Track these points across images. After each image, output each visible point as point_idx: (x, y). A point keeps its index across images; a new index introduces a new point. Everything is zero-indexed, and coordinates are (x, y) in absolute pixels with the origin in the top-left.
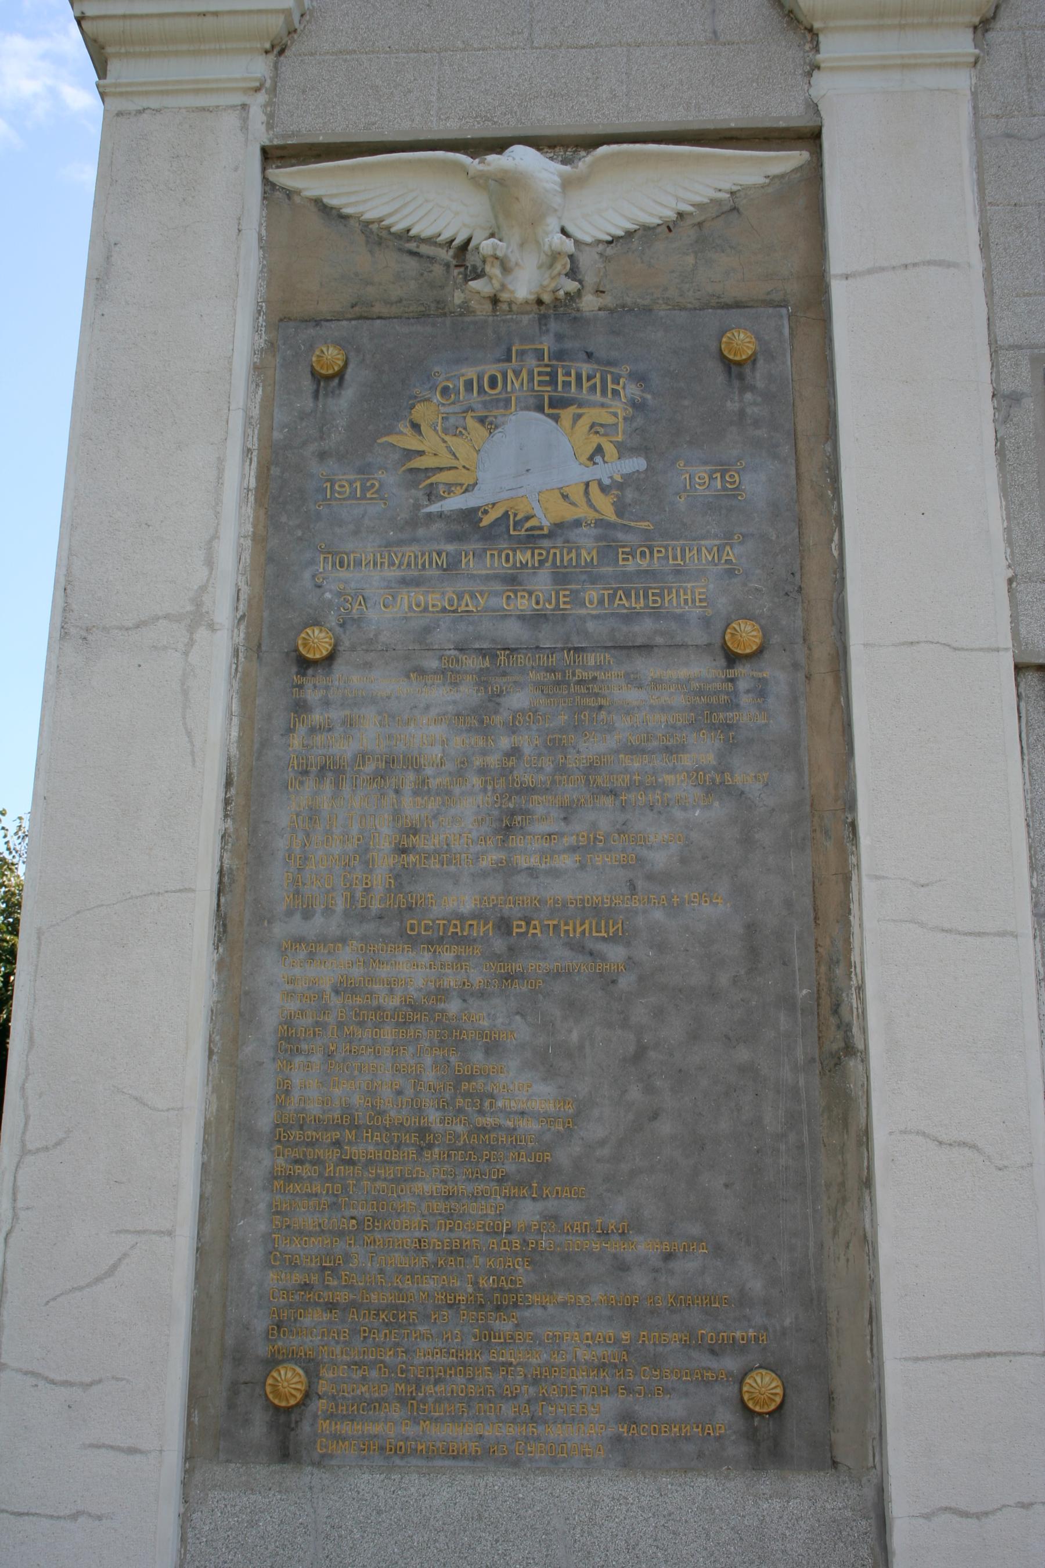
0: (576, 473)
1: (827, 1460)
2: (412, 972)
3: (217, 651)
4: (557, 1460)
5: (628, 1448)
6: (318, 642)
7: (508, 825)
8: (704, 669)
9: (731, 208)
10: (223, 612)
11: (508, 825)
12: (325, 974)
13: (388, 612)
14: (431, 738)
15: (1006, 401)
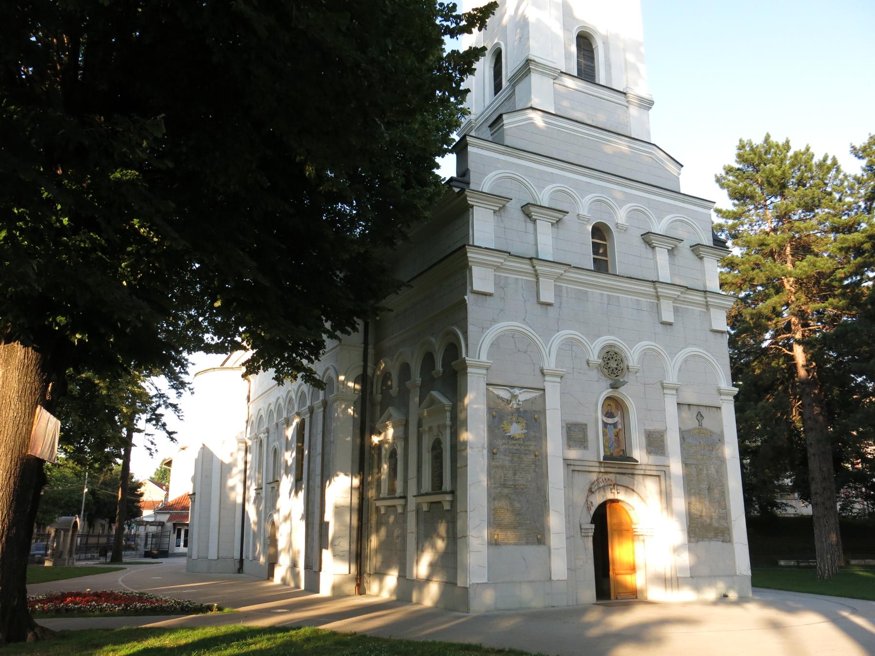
0: (520, 432)
1: (544, 544)
2: (506, 491)
3: (485, 452)
4: (521, 544)
5: (527, 543)
6: (495, 451)
7: (515, 474)
8: (532, 457)
9: (535, 398)
10: (486, 446)
11: (515, 474)
12: (497, 491)
13: (502, 448)
14: (507, 464)
15: (562, 427)
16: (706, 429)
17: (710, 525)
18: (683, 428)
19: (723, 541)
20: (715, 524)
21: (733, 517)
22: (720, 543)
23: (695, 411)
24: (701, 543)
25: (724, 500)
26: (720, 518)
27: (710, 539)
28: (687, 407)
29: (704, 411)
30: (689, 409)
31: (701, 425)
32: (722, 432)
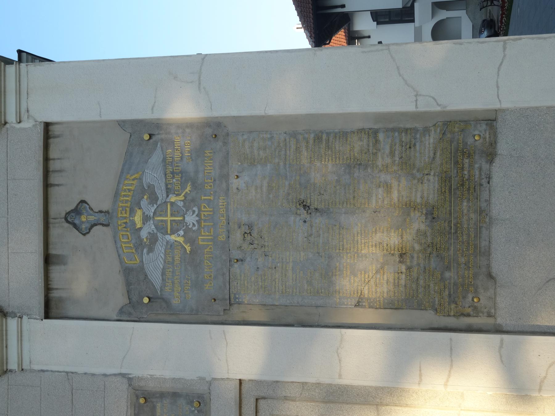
16: (117, 195)
17: (431, 214)
18: (119, 298)
19: (491, 155)
20: (429, 190)
21: (405, 105)
22: (498, 172)
23: (65, 238)
24: (498, 265)
25: (344, 135)
26: (407, 166)
27: (483, 214)
28: (56, 271)
29: (61, 206)
30: (61, 260)
31: (106, 219)
32: (122, 124)
